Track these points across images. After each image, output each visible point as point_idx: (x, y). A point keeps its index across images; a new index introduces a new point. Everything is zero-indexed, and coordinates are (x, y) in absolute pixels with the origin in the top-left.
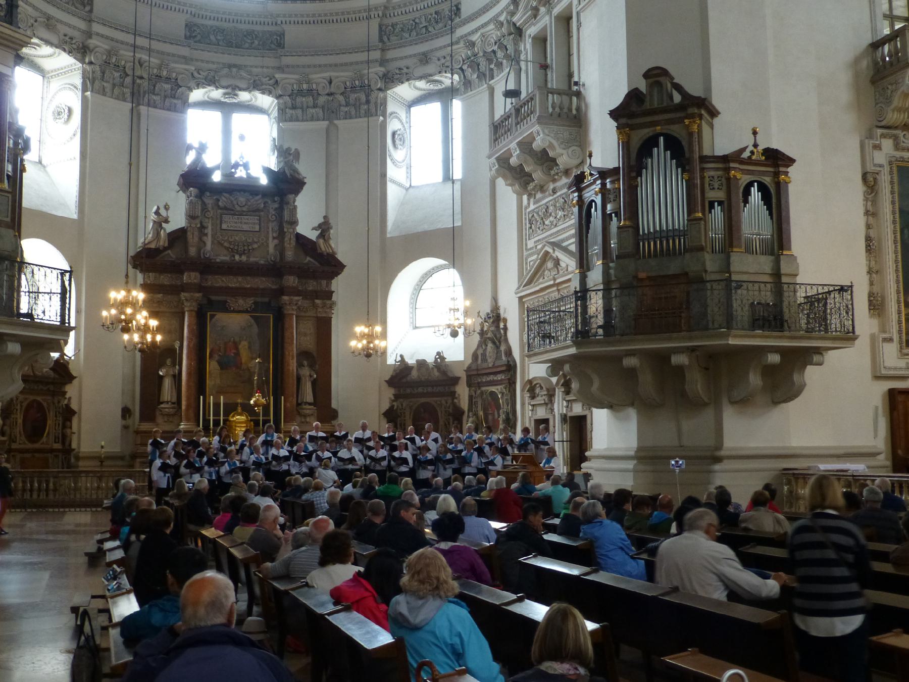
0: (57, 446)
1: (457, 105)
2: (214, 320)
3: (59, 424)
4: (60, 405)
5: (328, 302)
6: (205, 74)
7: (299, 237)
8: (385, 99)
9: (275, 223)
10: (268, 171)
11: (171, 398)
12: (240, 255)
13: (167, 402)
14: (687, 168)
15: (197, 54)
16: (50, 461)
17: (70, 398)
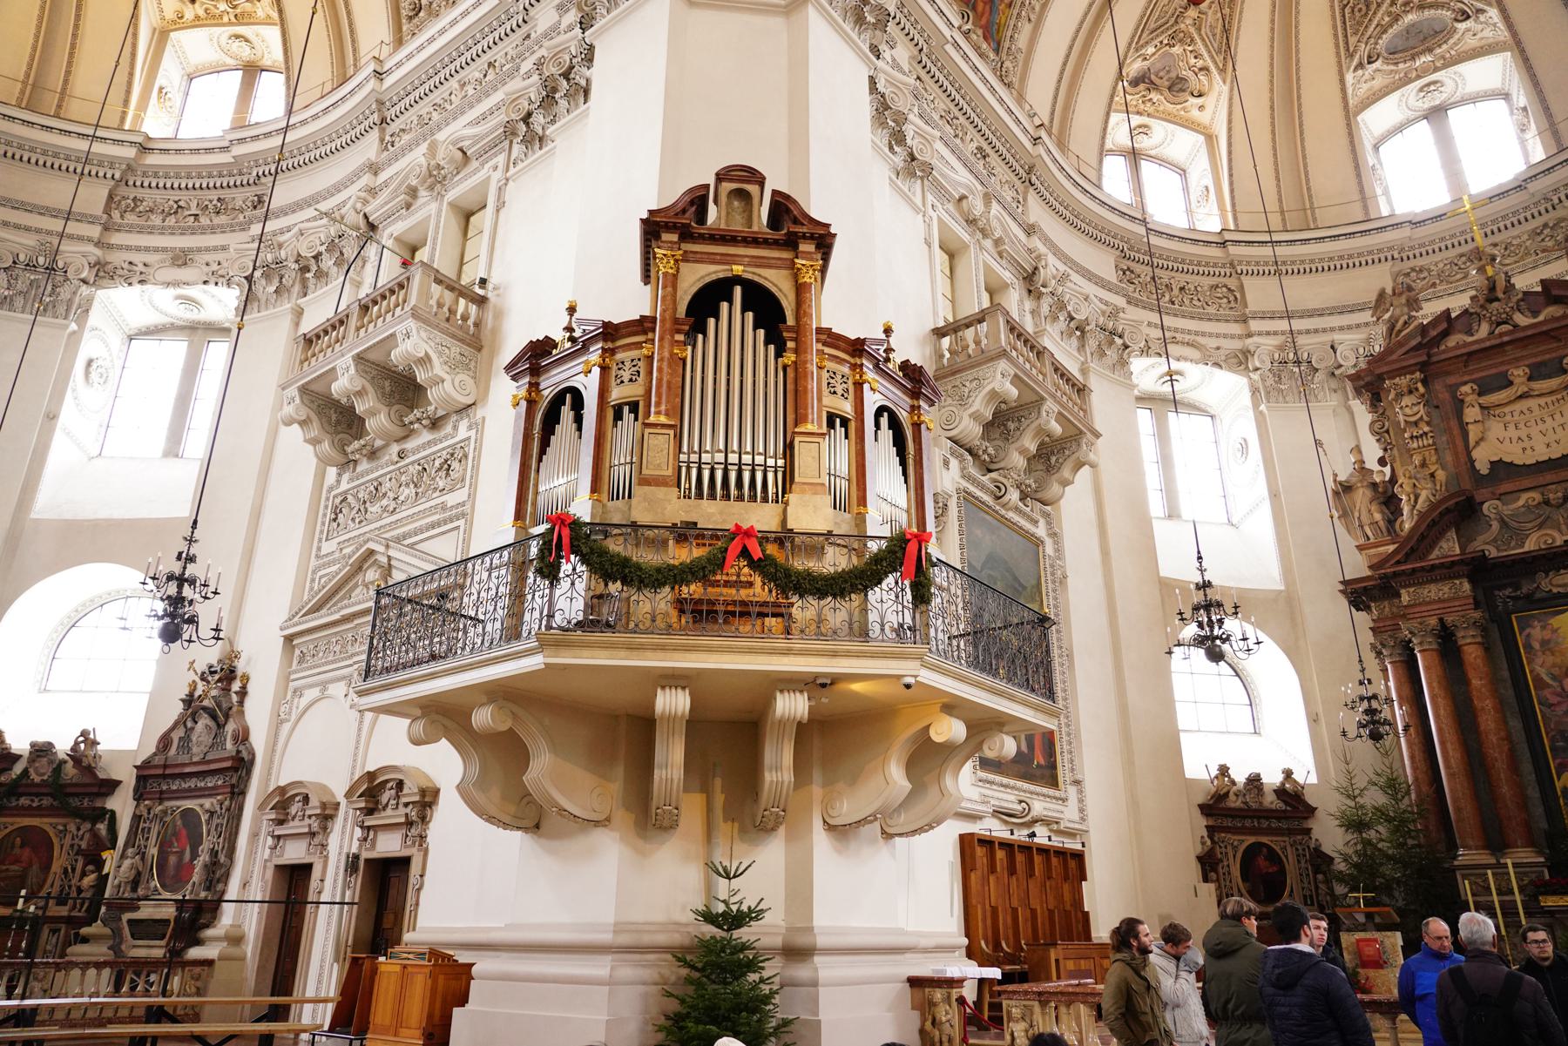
1: (217, 353)
8: (90, 301)
14: (790, 344)
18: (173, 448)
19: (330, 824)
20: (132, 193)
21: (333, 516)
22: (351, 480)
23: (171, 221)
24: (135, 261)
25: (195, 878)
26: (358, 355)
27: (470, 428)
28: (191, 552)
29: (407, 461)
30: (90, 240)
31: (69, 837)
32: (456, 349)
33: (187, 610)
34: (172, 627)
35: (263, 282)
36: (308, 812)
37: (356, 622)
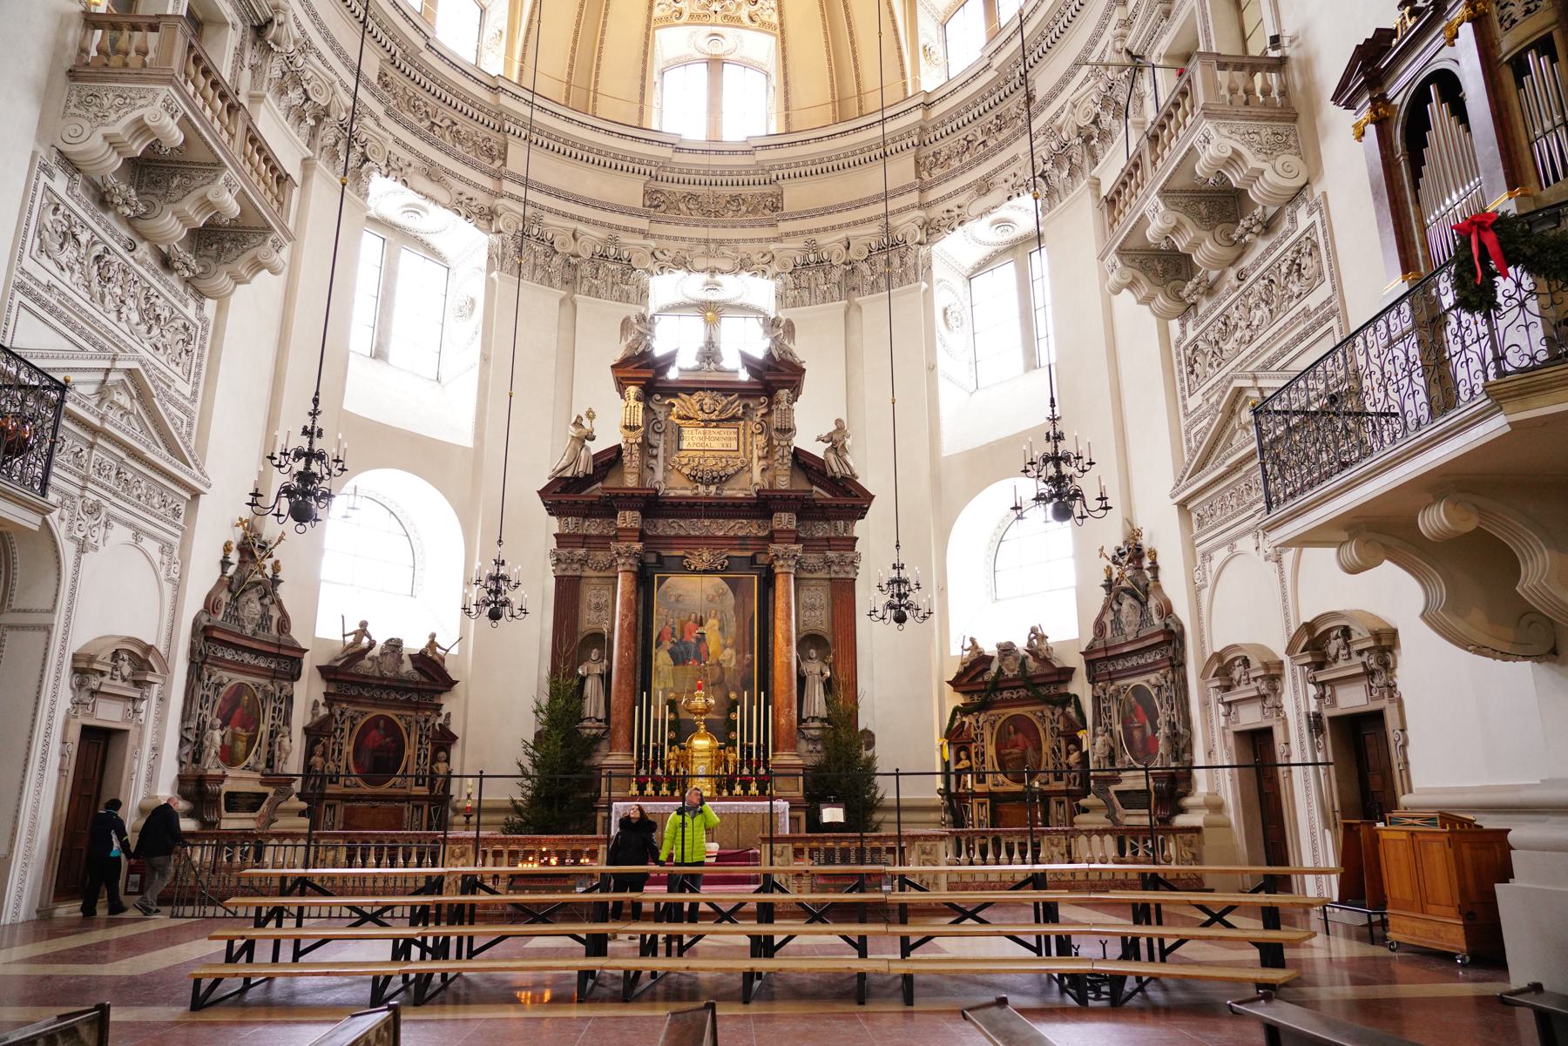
0: (423, 791)
2: (663, 587)
3: (426, 756)
4: (429, 724)
5: (850, 554)
6: (673, 255)
7: (798, 454)
8: (929, 258)
9: (759, 437)
10: (748, 361)
11: (597, 711)
12: (708, 485)
13: (590, 718)
15: (658, 229)
16: (406, 814)
17: (448, 715)
18: (1031, 364)
19: (1278, 685)
20: (930, 150)
21: (1189, 369)
22: (1196, 325)
23: (966, 158)
24: (950, 208)
25: (1161, 750)
26: (1162, 189)
27: (1311, 212)
28: (1057, 431)
29: (1249, 281)
30: (914, 207)
31: (1048, 721)
32: (1266, 131)
33: (1071, 487)
34: (1061, 507)
35: (1056, 171)
36: (1252, 675)
37: (1246, 468)
